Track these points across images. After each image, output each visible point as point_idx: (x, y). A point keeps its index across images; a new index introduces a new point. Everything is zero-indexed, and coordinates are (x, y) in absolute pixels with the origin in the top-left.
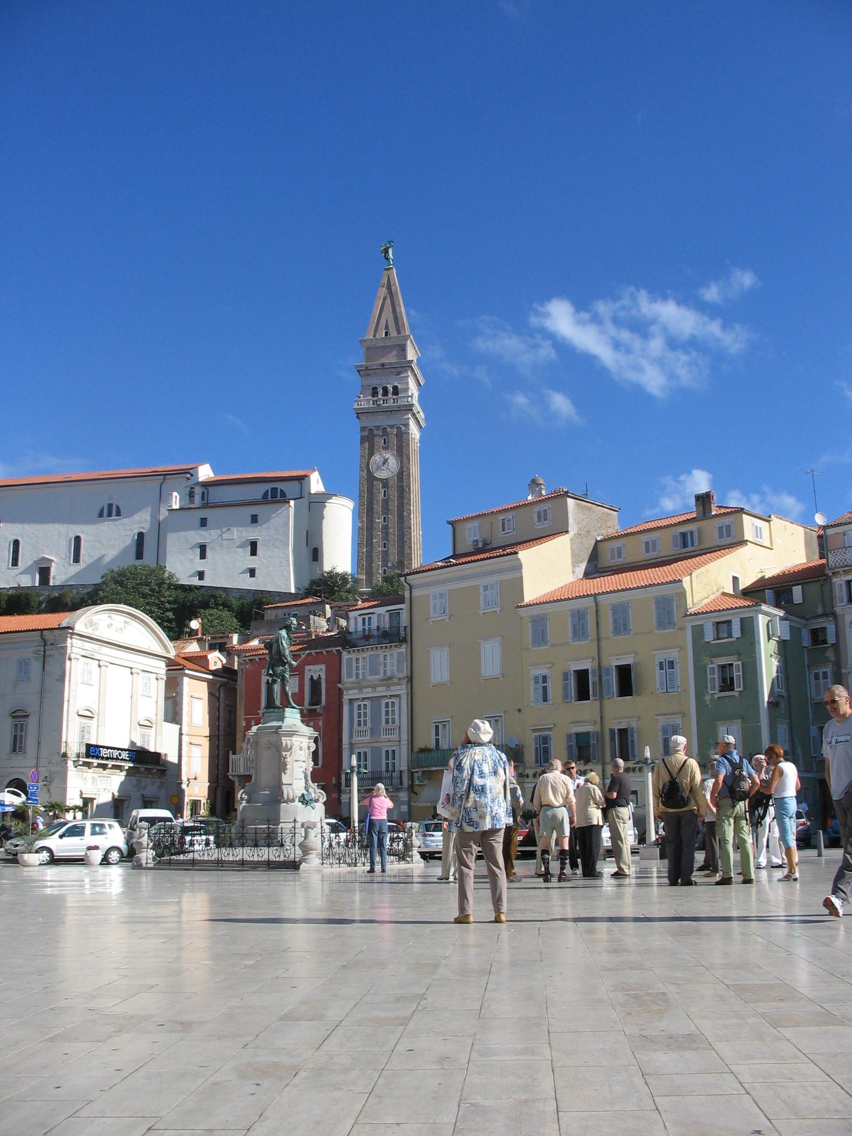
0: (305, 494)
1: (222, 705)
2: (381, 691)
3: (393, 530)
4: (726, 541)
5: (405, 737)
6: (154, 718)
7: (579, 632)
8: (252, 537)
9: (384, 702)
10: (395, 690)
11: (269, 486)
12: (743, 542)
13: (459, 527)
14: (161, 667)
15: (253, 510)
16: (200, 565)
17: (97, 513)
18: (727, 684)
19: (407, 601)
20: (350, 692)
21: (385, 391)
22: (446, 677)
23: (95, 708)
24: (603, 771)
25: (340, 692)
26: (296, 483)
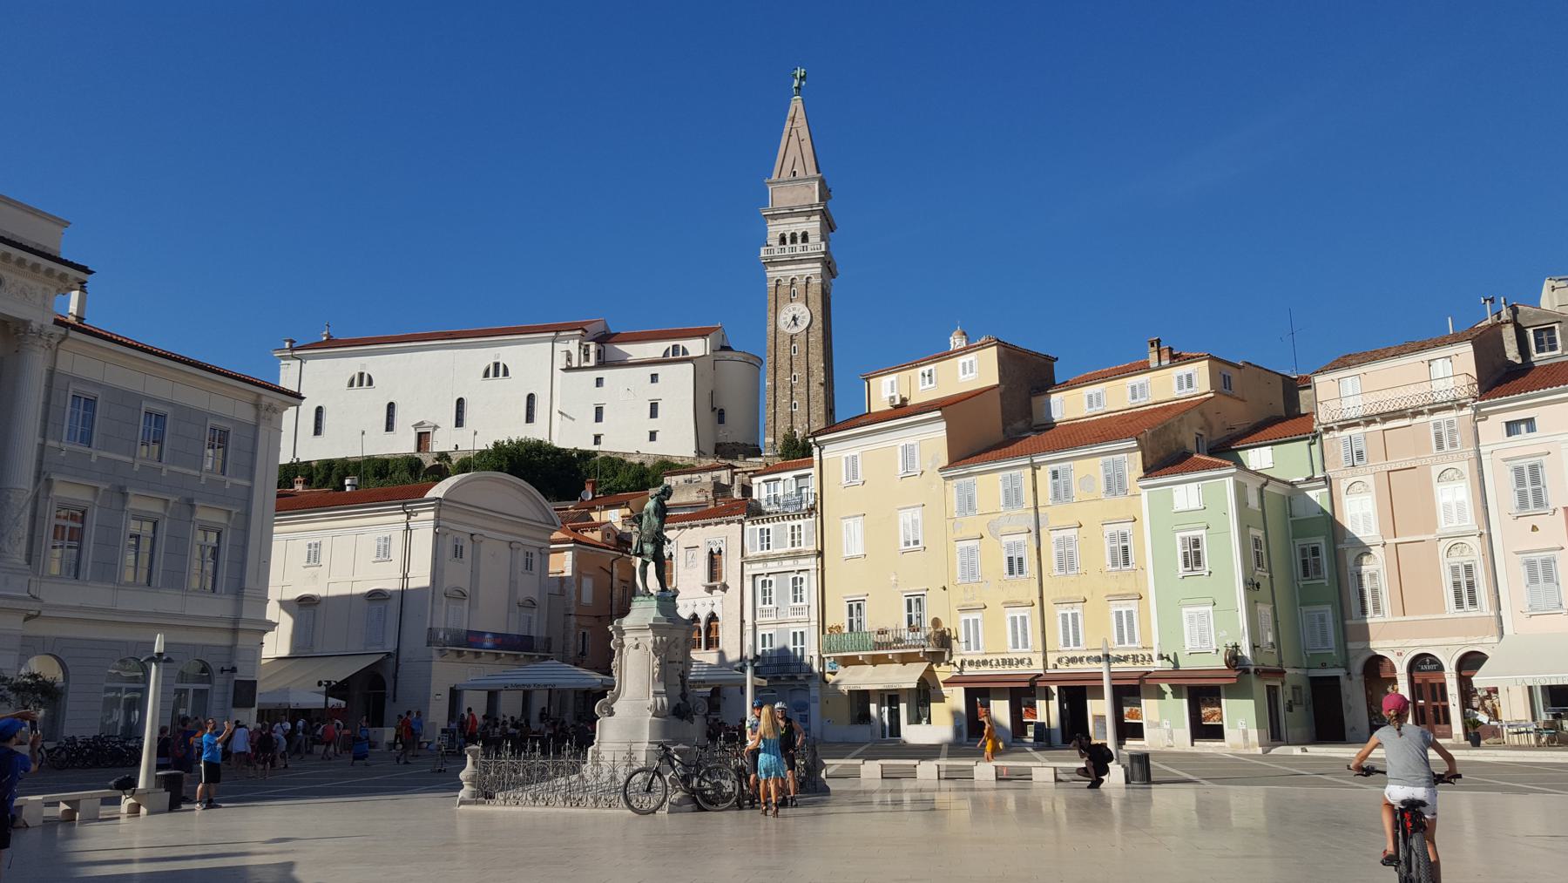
1: (615, 580)
5: (814, 617)
6: (536, 597)
7: (1012, 498)
9: (792, 576)
11: (669, 344)
16: (598, 428)
17: (482, 374)
18: (1194, 558)
19: (816, 463)
20: (755, 566)
24: (1045, 660)
26: (700, 341)
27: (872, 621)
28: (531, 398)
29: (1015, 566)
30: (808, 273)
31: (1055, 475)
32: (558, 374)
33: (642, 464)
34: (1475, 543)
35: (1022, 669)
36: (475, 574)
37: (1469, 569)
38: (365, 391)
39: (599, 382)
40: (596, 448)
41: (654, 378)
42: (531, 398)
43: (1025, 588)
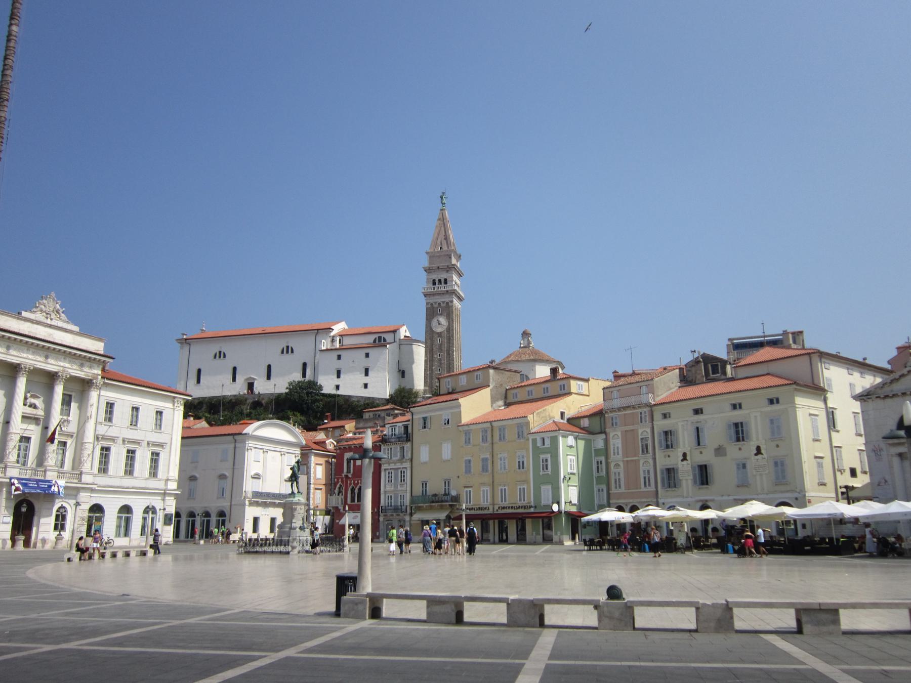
0: (397, 340)
2: (398, 465)
3: (445, 362)
4: (563, 392)
5: (409, 489)
7: (484, 440)
8: (366, 366)
10: (405, 465)
12: (570, 393)
13: (442, 381)
14: (298, 451)
15: (367, 351)
16: (337, 382)
21: (440, 281)
22: (427, 459)
23: (261, 473)
25: (380, 465)
26: (392, 335)
27: (431, 491)
28: (305, 365)
29: (485, 469)
30: (447, 300)
31: (500, 430)
32: (318, 354)
33: (358, 401)
34: (651, 461)
35: (486, 512)
36: (264, 466)
37: (649, 471)
38: (222, 360)
39: (339, 357)
40: (339, 392)
41: (367, 355)
42: (305, 365)
43: (487, 478)
